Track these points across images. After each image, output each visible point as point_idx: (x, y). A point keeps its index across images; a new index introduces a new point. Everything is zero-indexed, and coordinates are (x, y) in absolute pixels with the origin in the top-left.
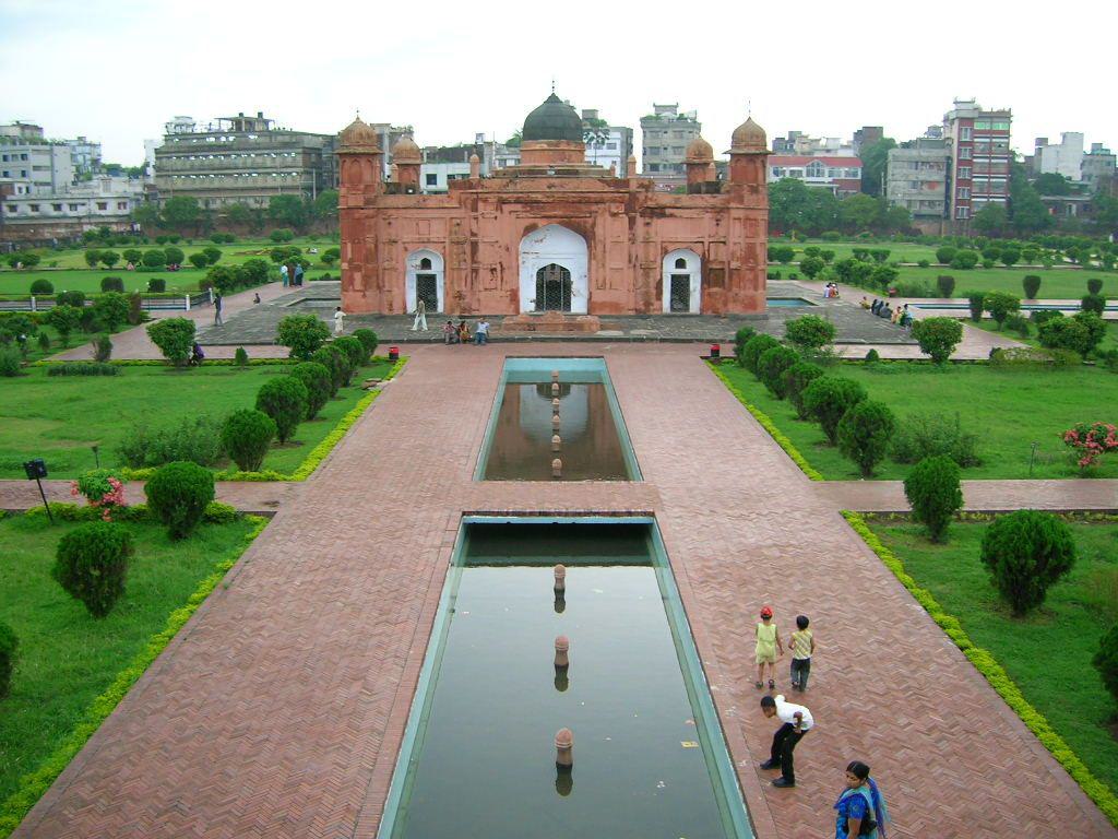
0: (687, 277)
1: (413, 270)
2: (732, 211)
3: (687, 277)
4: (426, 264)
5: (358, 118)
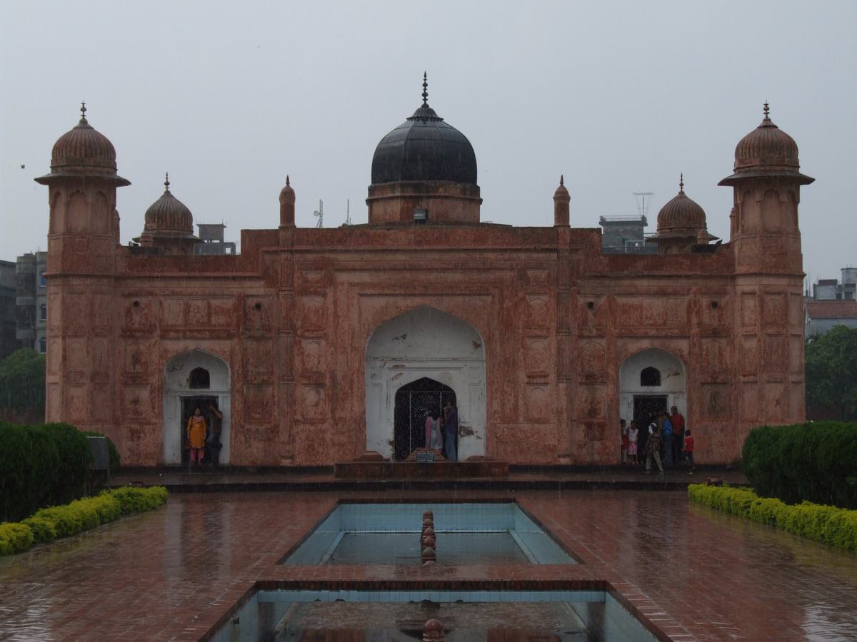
1: (180, 385)
2: (740, 281)
4: (200, 378)
5: (84, 122)
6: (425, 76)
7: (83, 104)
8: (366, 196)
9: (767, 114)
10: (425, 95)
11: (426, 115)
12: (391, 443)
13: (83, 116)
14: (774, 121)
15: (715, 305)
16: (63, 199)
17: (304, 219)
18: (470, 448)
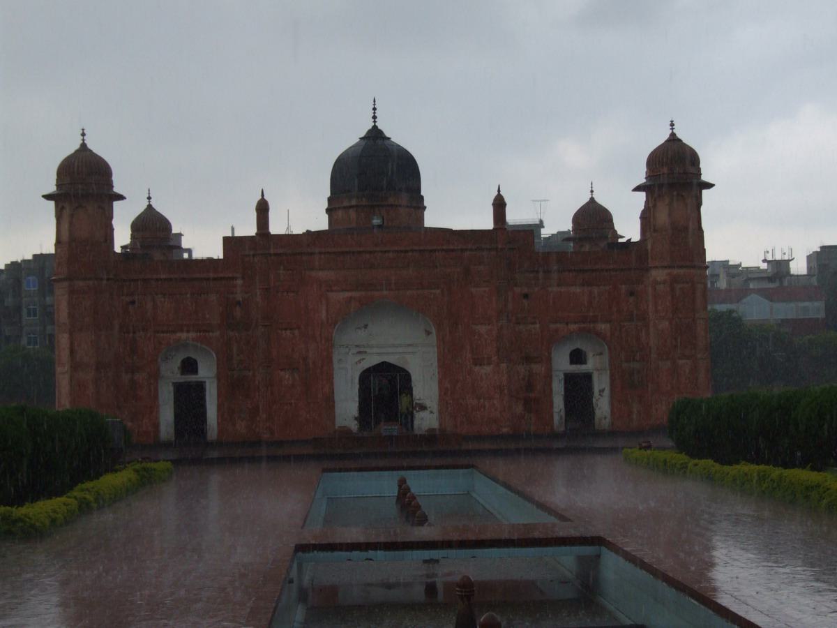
0: (588, 377)
1: (171, 372)
3: (588, 377)
4: (189, 366)
5: (84, 146)
6: (374, 101)
7: (83, 130)
8: (326, 205)
9: (672, 129)
10: (374, 117)
11: (375, 135)
12: (356, 419)
13: (83, 140)
14: (679, 135)
15: (632, 294)
16: (67, 212)
17: (277, 227)
18: (426, 421)
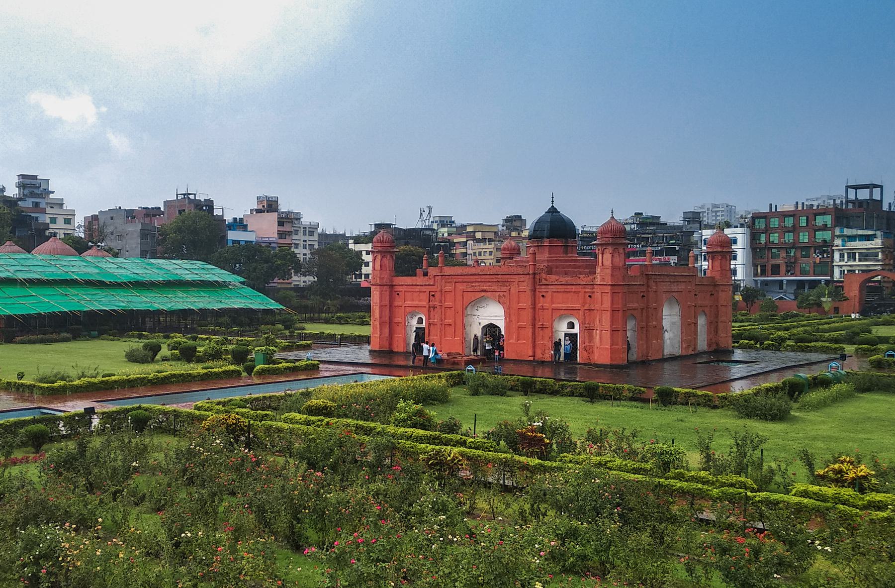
1: (414, 323)
